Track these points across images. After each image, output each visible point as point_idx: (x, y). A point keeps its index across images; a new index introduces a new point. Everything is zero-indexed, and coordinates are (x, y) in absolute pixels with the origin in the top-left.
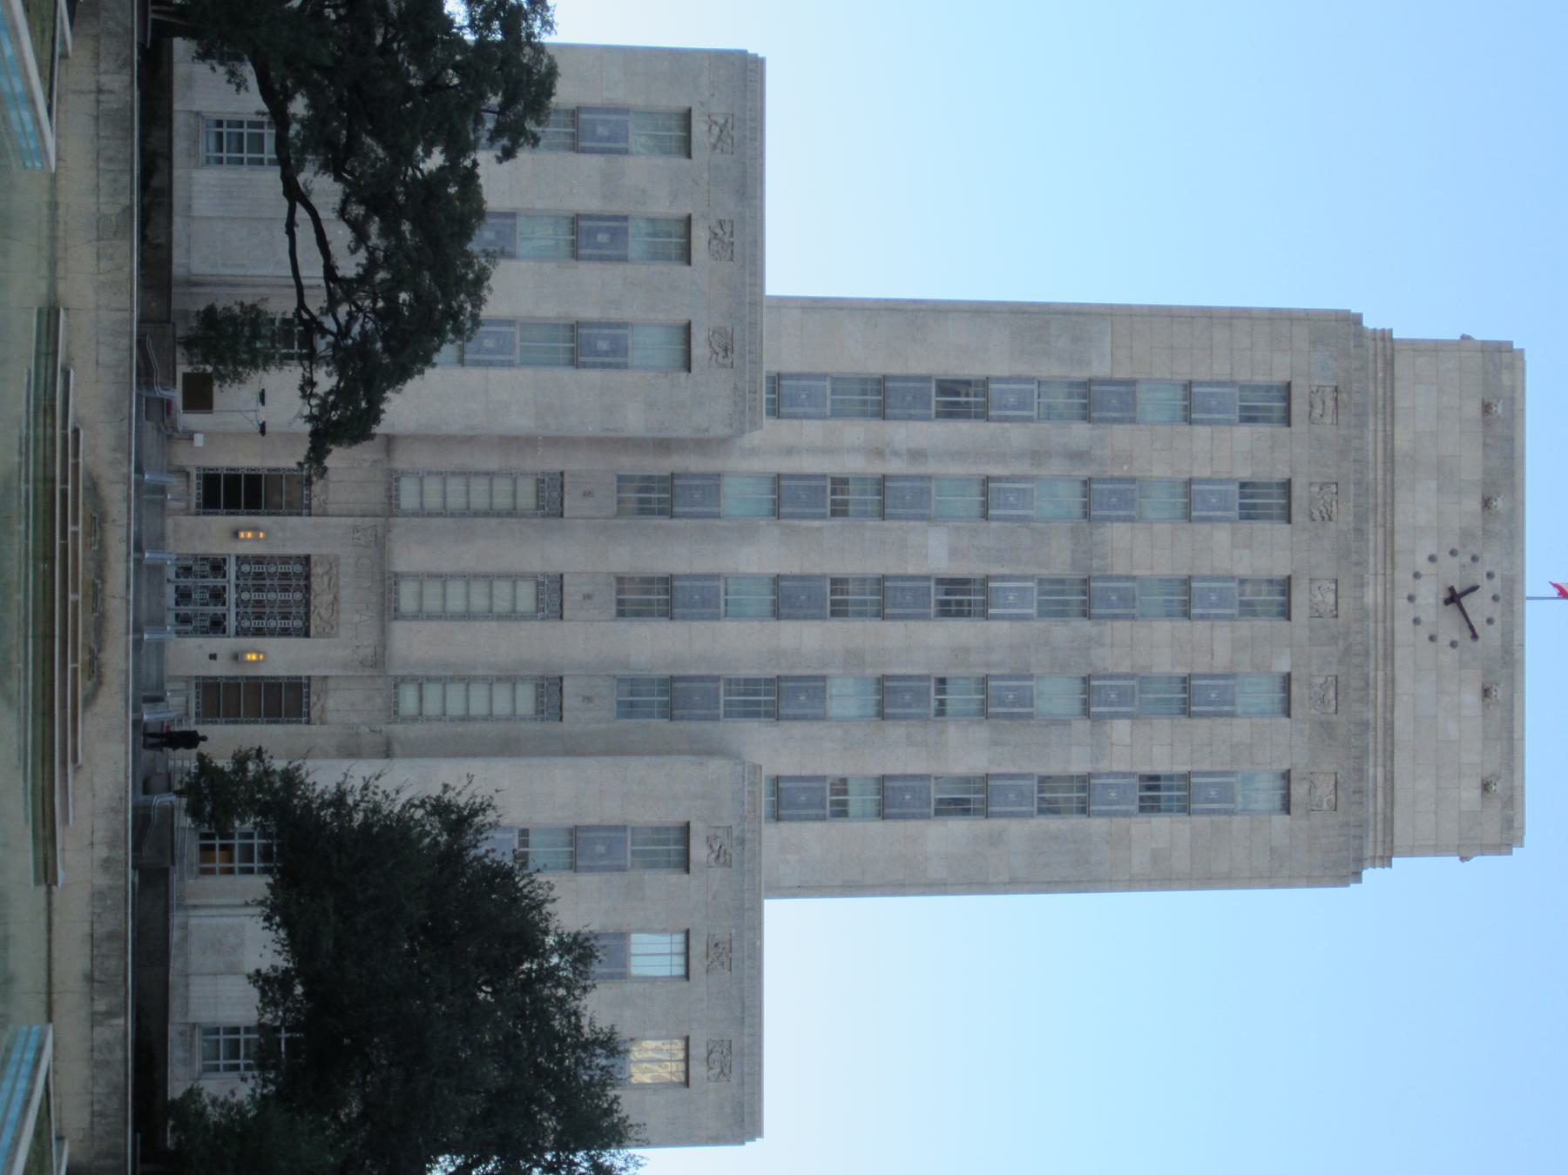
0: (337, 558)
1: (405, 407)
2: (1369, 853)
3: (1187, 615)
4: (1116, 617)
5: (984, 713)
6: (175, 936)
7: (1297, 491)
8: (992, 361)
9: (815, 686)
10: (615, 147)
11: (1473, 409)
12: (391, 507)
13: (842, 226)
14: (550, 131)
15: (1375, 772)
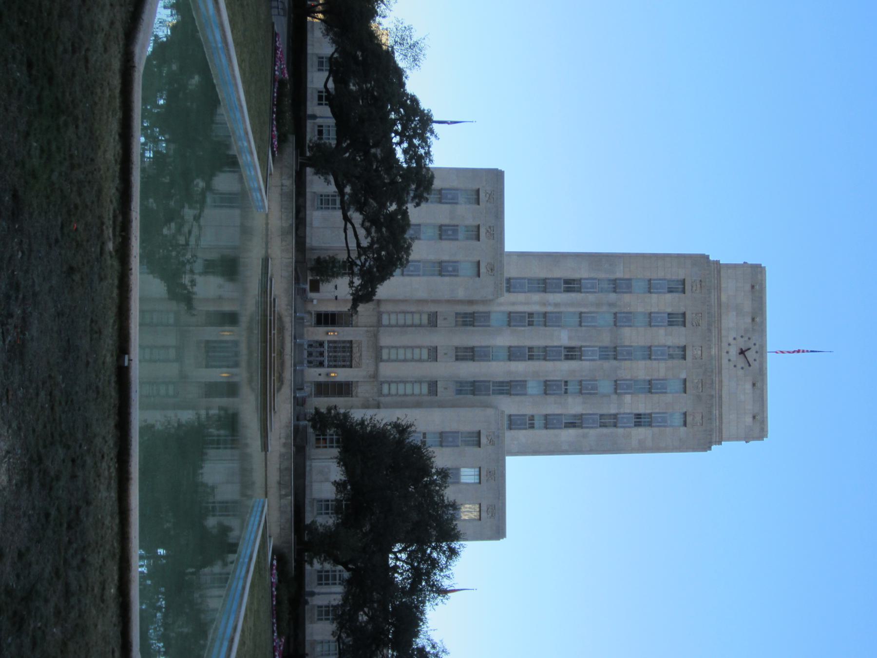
1: (383, 291)
2: (714, 440)
3: (650, 358)
4: (625, 360)
5: (581, 393)
6: (308, 469)
7: (687, 316)
8: (582, 273)
9: (523, 384)
10: (454, 202)
11: (748, 287)
12: (379, 324)
13: (530, 227)
14: (431, 197)
15: (716, 412)
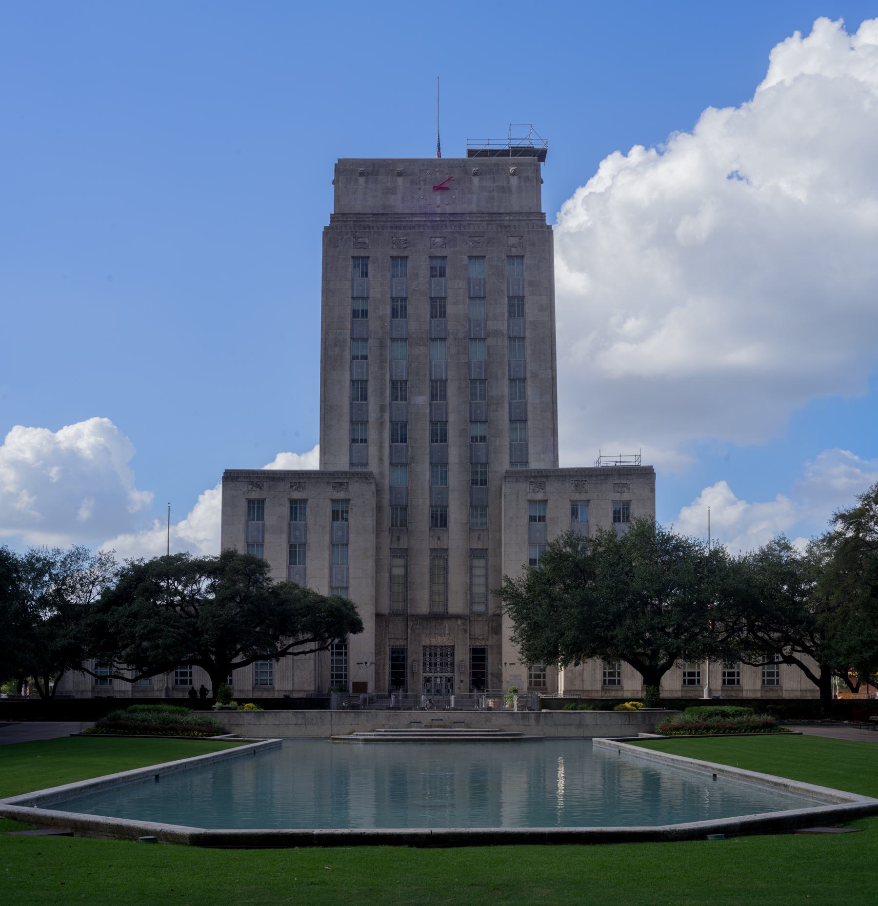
4: (446, 328)
7: (395, 254)
14: (255, 553)
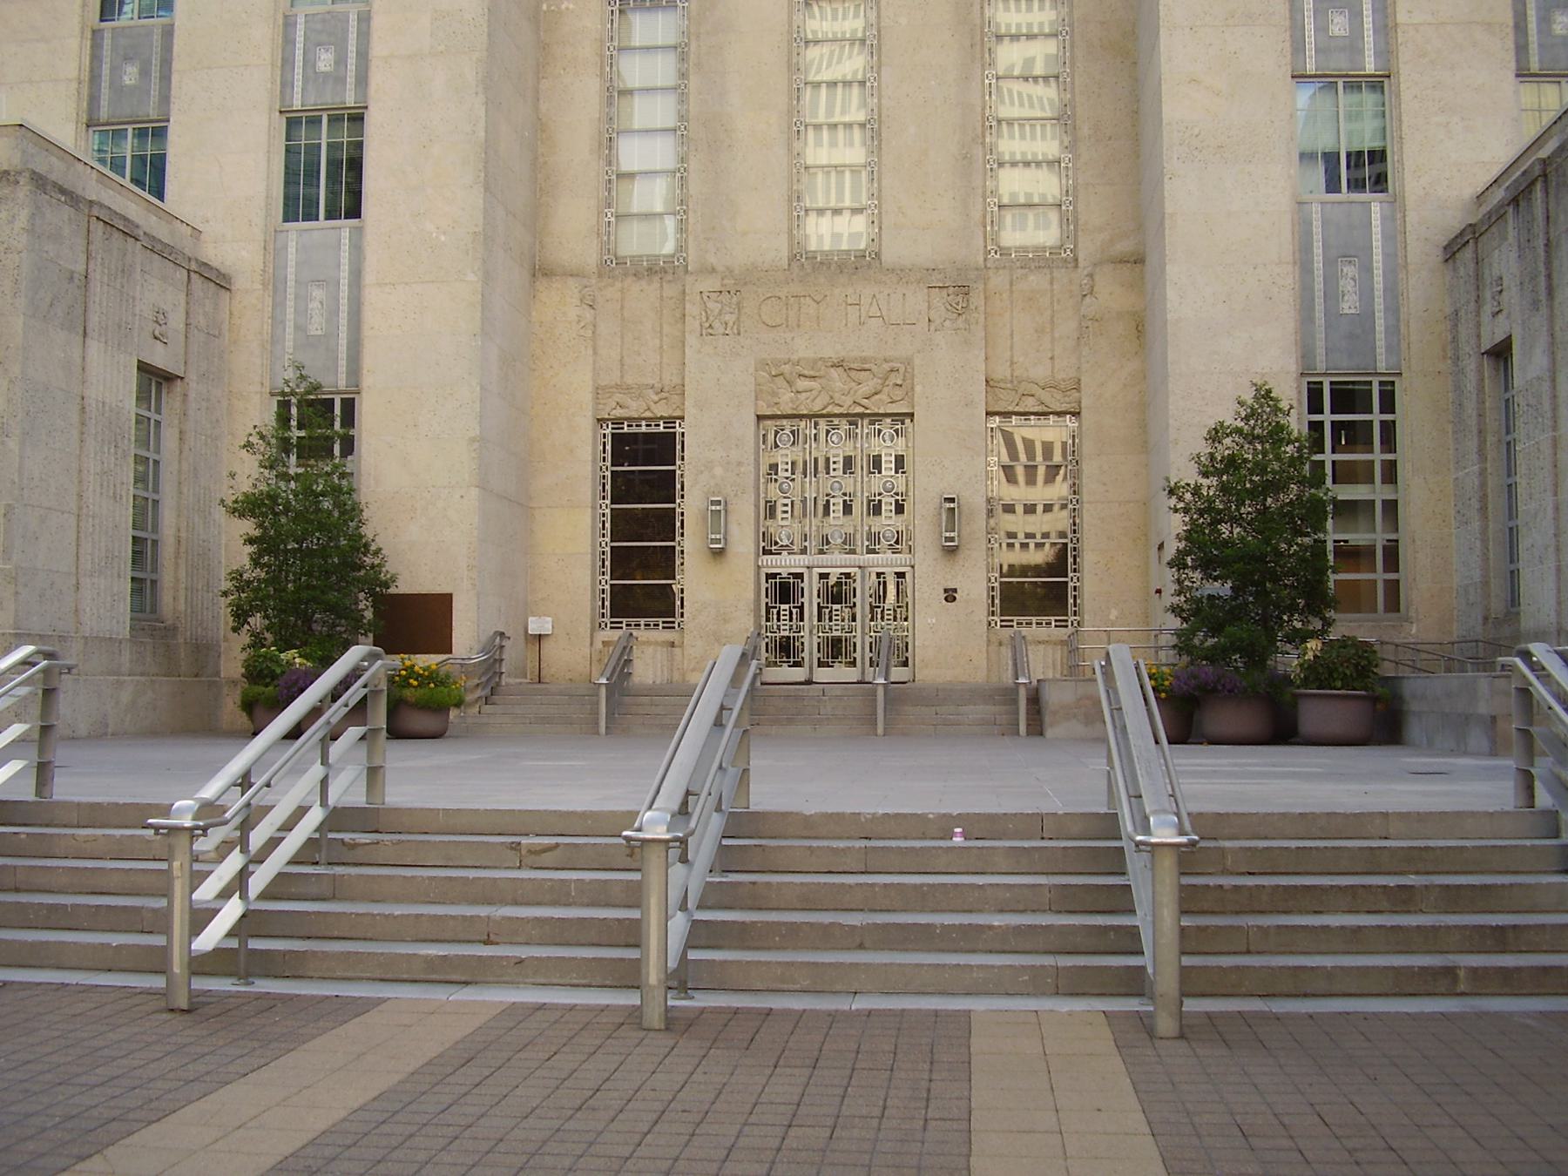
0: (763, 364)
